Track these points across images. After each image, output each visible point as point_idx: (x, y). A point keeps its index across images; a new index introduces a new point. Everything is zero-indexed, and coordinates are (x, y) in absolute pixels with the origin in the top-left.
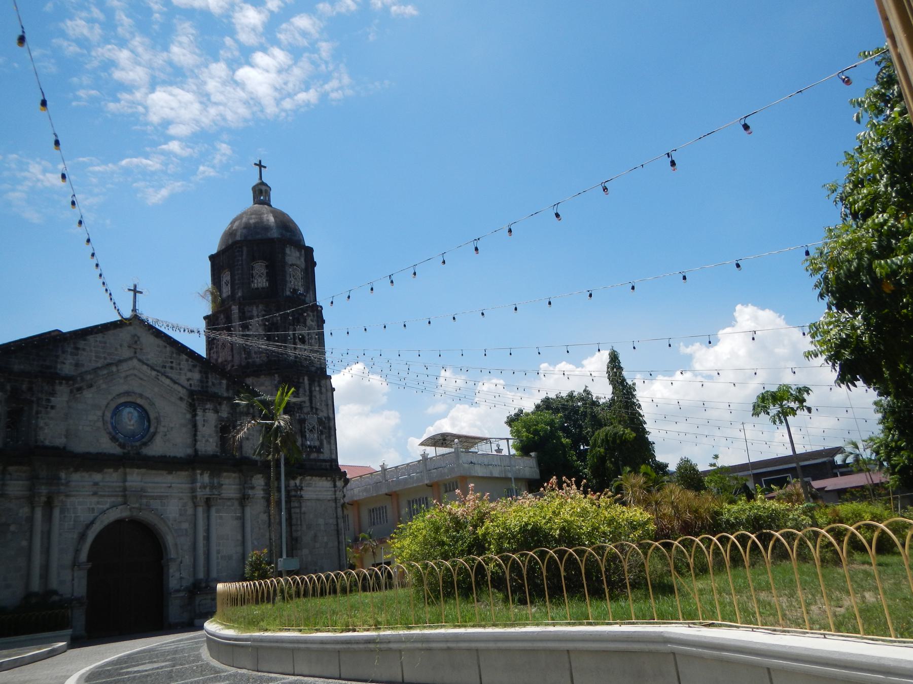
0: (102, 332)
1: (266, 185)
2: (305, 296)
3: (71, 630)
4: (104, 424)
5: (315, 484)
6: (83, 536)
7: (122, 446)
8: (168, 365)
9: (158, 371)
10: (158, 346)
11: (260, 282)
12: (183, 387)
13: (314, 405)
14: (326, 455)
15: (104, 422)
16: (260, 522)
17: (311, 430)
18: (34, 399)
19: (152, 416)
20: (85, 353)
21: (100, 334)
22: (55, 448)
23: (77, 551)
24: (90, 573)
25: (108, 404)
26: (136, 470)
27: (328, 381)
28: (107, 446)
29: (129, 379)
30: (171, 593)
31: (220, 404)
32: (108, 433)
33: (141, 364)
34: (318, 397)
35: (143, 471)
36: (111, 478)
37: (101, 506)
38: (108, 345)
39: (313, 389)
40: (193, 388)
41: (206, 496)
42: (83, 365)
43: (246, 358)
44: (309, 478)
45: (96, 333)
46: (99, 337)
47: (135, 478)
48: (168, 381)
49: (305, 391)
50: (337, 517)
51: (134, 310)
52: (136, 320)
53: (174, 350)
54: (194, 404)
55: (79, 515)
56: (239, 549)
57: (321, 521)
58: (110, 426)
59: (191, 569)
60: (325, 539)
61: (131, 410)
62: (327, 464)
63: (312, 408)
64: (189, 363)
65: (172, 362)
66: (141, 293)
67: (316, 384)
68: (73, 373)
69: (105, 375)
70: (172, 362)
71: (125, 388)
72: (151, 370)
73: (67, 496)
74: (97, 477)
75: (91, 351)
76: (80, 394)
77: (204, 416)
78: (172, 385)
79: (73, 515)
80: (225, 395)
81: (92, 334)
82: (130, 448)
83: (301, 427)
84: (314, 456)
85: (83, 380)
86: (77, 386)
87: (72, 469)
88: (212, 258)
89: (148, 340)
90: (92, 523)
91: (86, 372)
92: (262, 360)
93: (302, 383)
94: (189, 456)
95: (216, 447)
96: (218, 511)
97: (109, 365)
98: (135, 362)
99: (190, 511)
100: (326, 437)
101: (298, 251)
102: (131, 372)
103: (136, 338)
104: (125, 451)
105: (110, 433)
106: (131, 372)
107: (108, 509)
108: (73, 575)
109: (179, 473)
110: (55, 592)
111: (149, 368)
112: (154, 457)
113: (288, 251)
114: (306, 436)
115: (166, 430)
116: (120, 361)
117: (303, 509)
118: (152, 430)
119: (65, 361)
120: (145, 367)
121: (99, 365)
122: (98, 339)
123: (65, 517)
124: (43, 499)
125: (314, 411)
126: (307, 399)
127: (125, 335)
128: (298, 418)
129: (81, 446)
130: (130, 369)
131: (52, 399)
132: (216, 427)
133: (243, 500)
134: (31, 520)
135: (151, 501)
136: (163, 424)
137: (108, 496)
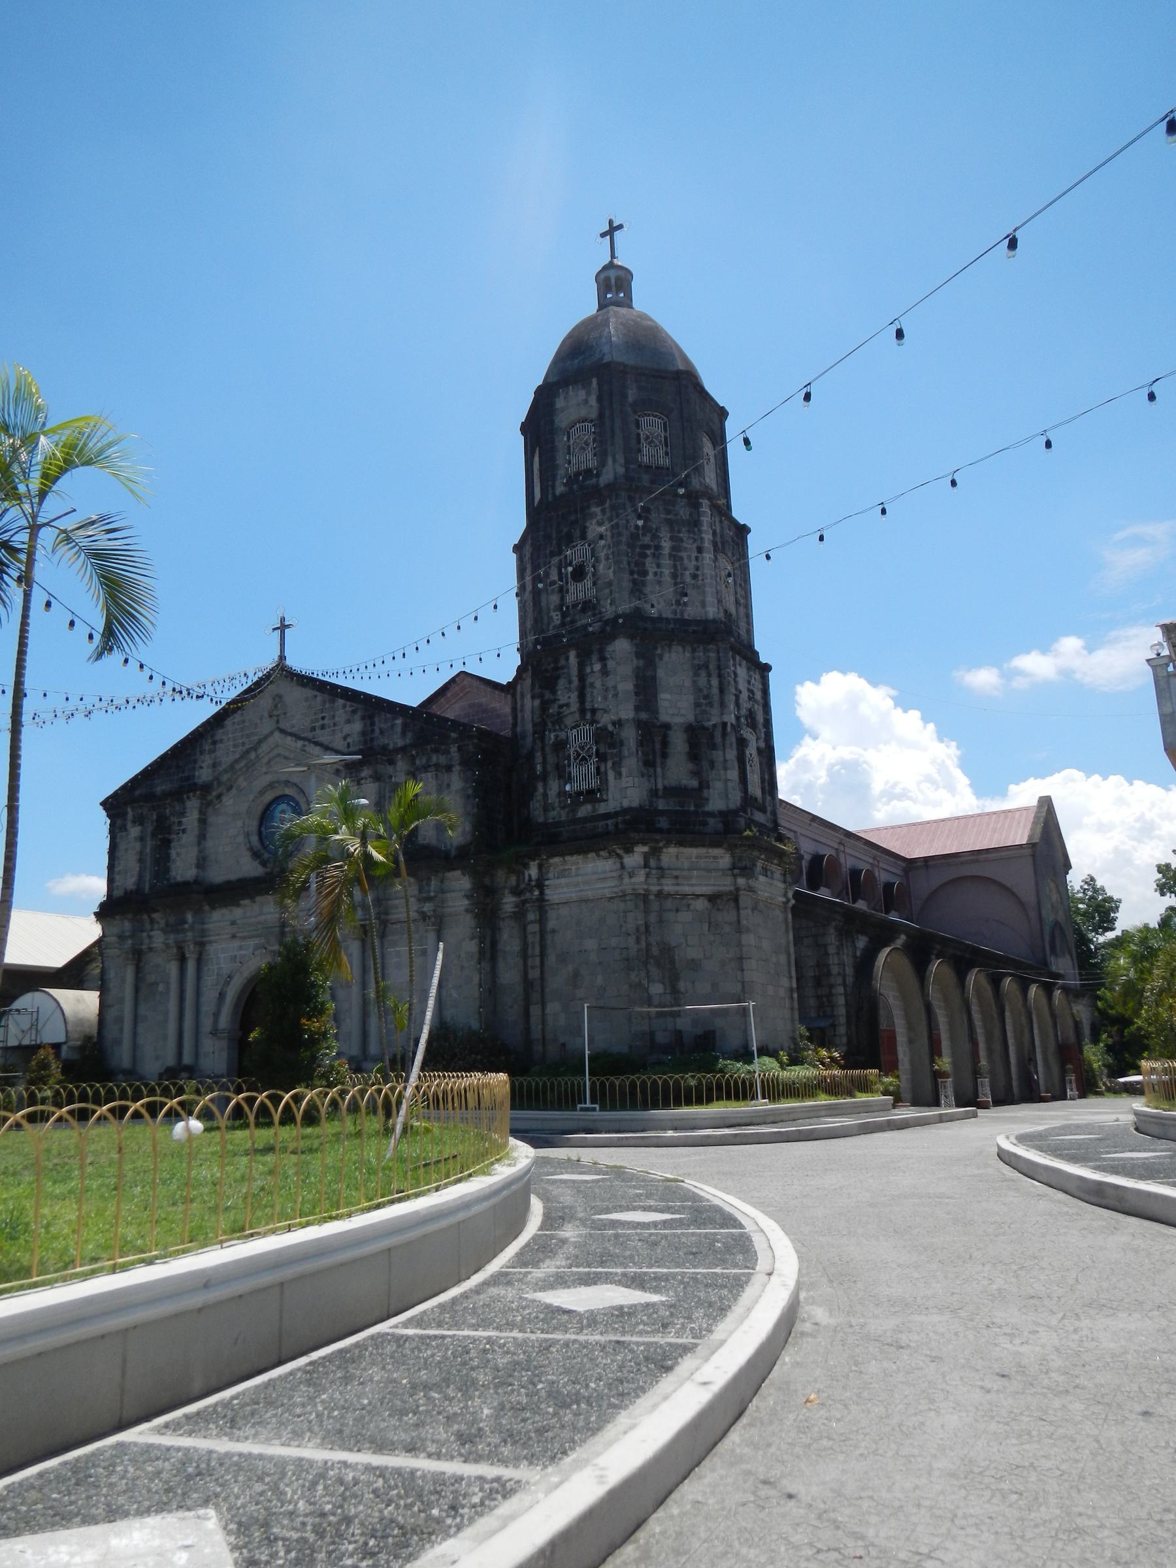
2: (598, 475)
5: (578, 869)
6: (222, 996)
7: (264, 864)
10: (307, 699)
13: (588, 706)
17: (584, 759)
20: (222, 746)
22: (186, 884)
23: (216, 1015)
28: (249, 868)
31: (392, 762)
34: (598, 684)
37: (243, 952)
39: (588, 670)
44: (556, 860)
46: (237, 717)
49: (570, 682)
51: (282, 657)
52: (282, 672)
53: (326, 696)
57: (591, 944)
58: (255, 839)
60: (599, 980)
62: (609, 822)
63: (582, 711)
65: (323, 718)
66: (288, 626)
67: (595, 658)
68: (210, 778)
71: (268, 778)
74: (237, 913)
80: (400, 743)
81: (229, 716)
83: (558, 756)
84: (584, 811)
85: (219, 784)
86: (214, 794)
87: (207, 908)
89: (294, 695)
93: (562, 668)
98: (277, 734)
100: (614, 764)
101: (584, 388)
102: (276, 752)
104: (268, 870)
105: (251, 849)
106: (276, 752)
116: (260, 742)
117: (551, 924)
120: (289, 738)
121: (237, 756)
125: (588, 716)
126: (574, 696)
127: (264, 702)
129: (218, 875)
130: (272, 750)
131: (183, 820)
137: (251, 937)
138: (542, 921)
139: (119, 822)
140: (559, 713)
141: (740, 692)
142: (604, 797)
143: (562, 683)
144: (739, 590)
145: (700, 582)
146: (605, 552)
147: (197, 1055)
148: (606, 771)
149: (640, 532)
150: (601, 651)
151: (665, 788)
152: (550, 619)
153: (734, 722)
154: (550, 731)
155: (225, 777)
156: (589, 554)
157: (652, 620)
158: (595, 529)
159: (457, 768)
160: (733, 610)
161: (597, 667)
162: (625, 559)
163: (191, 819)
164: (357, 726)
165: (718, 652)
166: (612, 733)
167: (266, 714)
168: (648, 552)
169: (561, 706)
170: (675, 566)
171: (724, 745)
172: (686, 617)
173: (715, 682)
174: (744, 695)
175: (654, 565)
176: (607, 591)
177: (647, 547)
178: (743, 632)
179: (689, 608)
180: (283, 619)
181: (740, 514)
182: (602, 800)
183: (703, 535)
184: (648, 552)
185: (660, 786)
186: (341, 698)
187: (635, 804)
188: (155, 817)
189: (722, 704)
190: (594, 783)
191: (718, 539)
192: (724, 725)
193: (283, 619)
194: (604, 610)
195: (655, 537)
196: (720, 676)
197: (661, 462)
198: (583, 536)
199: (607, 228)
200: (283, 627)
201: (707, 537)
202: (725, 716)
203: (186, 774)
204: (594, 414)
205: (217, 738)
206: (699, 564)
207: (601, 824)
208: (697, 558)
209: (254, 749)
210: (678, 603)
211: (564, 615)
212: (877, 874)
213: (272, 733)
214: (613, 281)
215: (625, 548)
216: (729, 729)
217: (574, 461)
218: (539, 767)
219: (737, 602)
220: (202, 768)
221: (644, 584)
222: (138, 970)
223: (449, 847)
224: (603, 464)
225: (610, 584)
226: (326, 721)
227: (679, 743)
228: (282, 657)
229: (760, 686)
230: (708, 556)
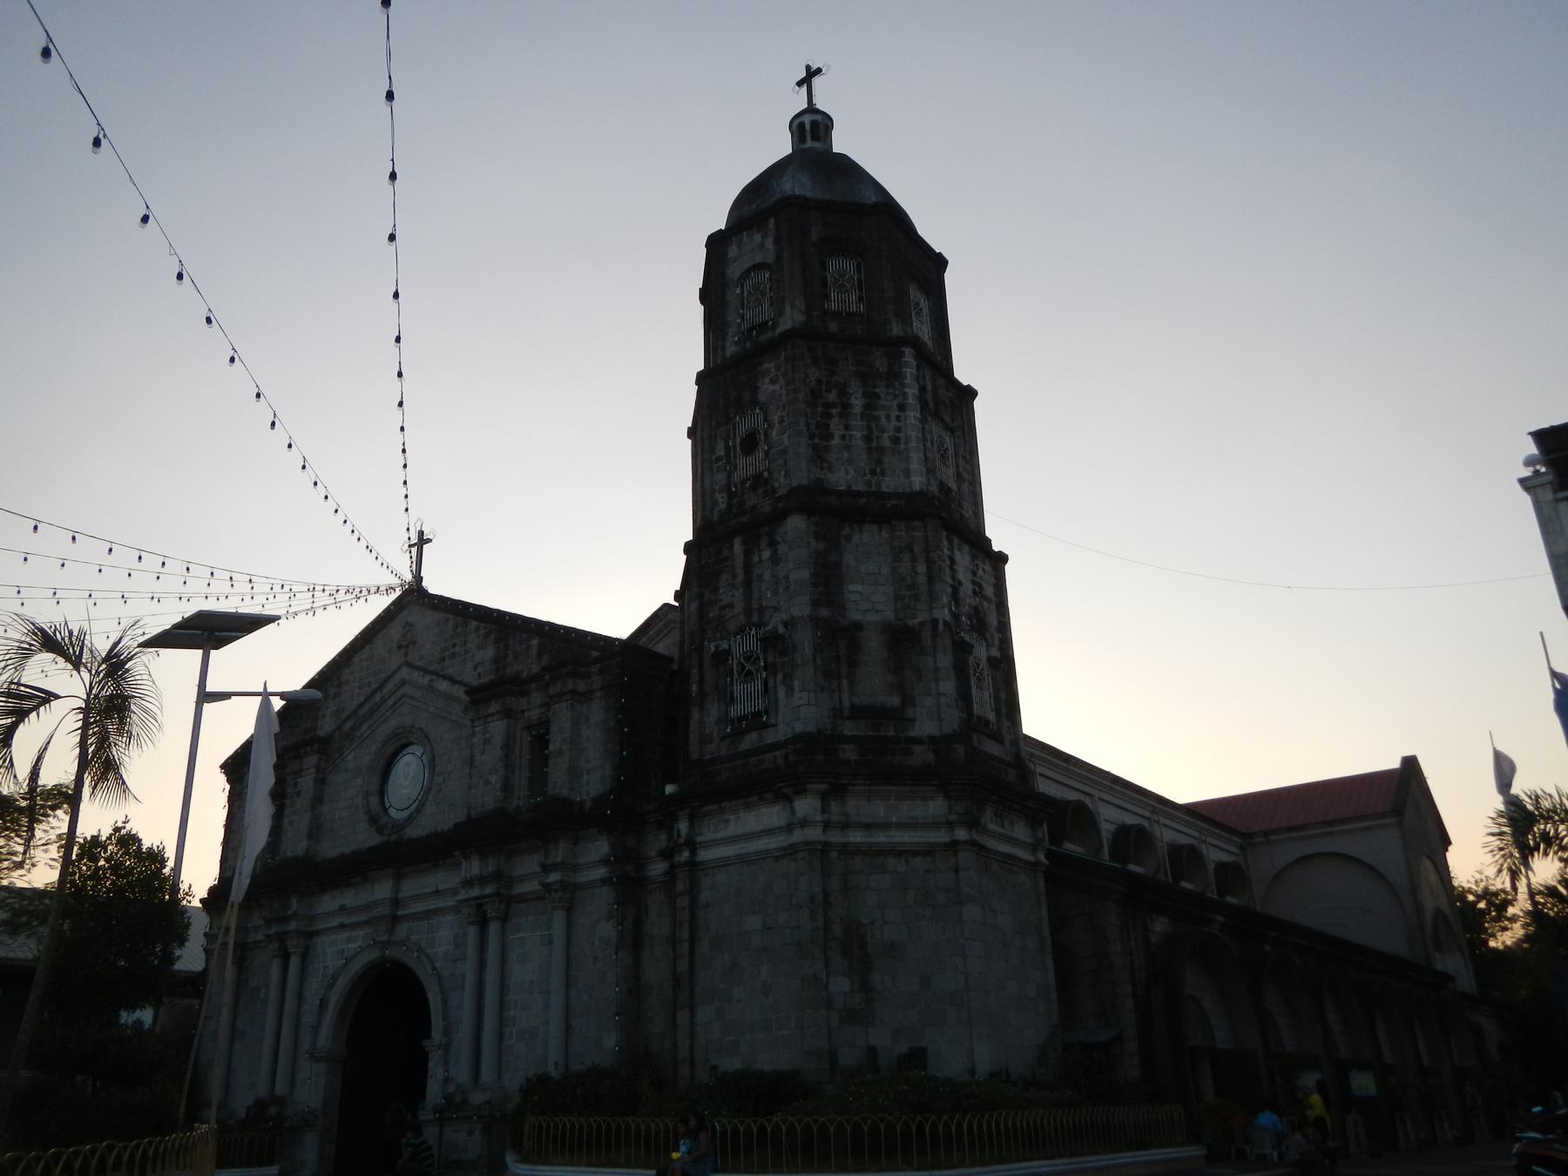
2: (774, 327)
3: (278, 1167)
7: (380, 830)
8: (448, 653)
17: (749, 673)
23: (316, 1028)
34: (767, 576)
39: (756, 559)
40: (484, 680)
45: (362, 647)
46: (365, 653)
47: (382, 890)
48: (443, 686)
49: (734, 576)
58: (374, 800)
62: (777, 753)
63: (748, 610)
65: (454, 645)
67: (763, 542)
71: (392, 723)
72: (423, 676)
80: (535, 669)
84: (750, 740)
95: (507, 787)
98: (405, 673)
100: (784, 676)
104: (385, 838)
120: (416, 673)
121: (362, 699)
125: (755, 618)
126: (738, 593)
127: (394, 631)
129: (330, 849)
131: (299, 780)
138: (693, 892)
141: (960, 583)
142: (773, 721)
143: (725, 578)
144: (961, 462)
145: (903, 446)
146: (779, 414)
147: (292, 1083)
148: (775, 687)
149: (824, 388)
151: (853, 706)
152: (715, 503)
153: (948, 617)
154: (710, 642)
156: (761, 418)
157: (839, 494)
158: (767, 388)
159: (598, 694)
160: (954, 487)
161: (766, 554)
162: (803, 419)
164: (490, 652)
165: (926, 531)
166: (783, 637)
168: (834, 411)
169: (723, 608)
170: (869, 428)
171: (934, 649)
172: (884, 489)
173: (922, 568)
174: (967, 588)
175: (841, 427)
176: (781, 462)
177: (834, 405)
178: (968, 513)
179: (887, 479)
180: (421, 533)
181: (963, 373)
182: (766, 726)
183: (906, 390)
184: (834, 411)
185: (846, 702)
187: (811, 727)
189: (932, 597)
190: (760, 706)
191: (929, 396)
192: (935, 622)
193: (421, 533)
194: (777, 485)
195: (843, 393)
196: (928, 561)
197: (854, 308)
198: (754, 402)
199: (803, 74)
200: (422, 541)
201: (912, 391)
202: (935, 611)
204: (770, 259)
206: (901, 424)
207: (767, 756)
208: (898, 418)
209: (380, 688)
210: (873, 472)
211: (731, 496)
212: (1205, 852)
213: (399, 669)
214: (808, 127)
215: (803, 406)
216: (941, 626)
217: (748, 315)
218: (694, 688)
219: (959, 476)
221: (827, 449)
223: (585, 798)
224: (780, 313)
225: (785, 452)
226: (457, 649)
227: (873, 644)
228: (418, 578)
229: (993, 580)
230: (913, 415)
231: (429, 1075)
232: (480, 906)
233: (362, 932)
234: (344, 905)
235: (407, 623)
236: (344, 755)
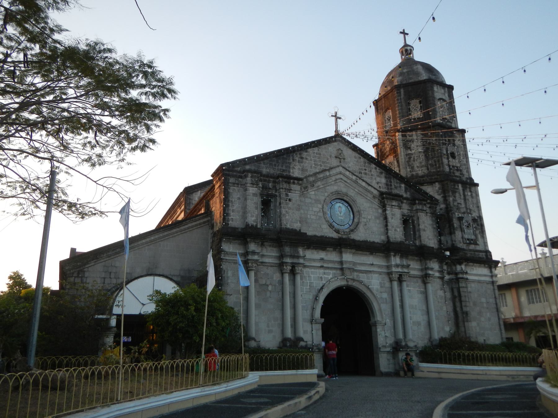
0: (317, 146)
1: (410, 46)
2: (451, 123)
4: (324, 215)
6: (316, 299)
7: (337, 231)
9: (357, 176)
10: (355, 157)
11: (417, 114)
12: (375, 188)
14: (480, 247)
15: (324, 213)
16: (438, 297)
17: (468, 227)
18: (277, 194)
19: (355, 210)
20: (307, 162)
21: (316, 148)
24: (323, 325)
25: (325, 199)
26: (349, 250)
27: (476, 187)
29: (338, 181)
30: (380, 348)
31: (402, 203)
32: (326, 221)
33: (345, 170)
34: (470, 199)
35: (354, 251)
36: (332, 256)
37: (326, 276)
38: (322, 156)
39: (466, 194)
40: (381, 190)
41: (399, 273)
42: (307, 170)
43: (410, 172)
45: (314, 147)
46: (316, 150)
47: (348, 257)
48: (364, 184)
50: (495, 298)
52: (338, 138)
53: (366, 161)
54: (384, 201)
55: (312, 281)
56: (425, 317)
57: (484, 300)
59: (392, 330)
61: (341, 205)
63: (467, 209)
64: (377, 170)
67: (468, 190)
68: (300, 176)
69: (322, 177)
70: (365, 170)
71: (335, 188)
73: (305, 266)
74: (322, 255)
75: (311, 160)
76: (306, 191)
77: (391, 211)
78: (367, 186)
79: (308, 281)
80: (405, 196)
81: (311, 147)
82: (342, 233)
84: (472, 247)
87: (306, 247)
88: (376, 103)
89: (348, 153)
90: (322, 288)
91: (310, 176)
92: (424, 172)
93: (457, 189)
94: (384, 241)
96: (407, 286)
97: (324, 170)
98: (341, 169)
99: (387, 284)
100: (480, 232)
101: (443, 89)
103: (340, 152)
104: (340, 235)
107: (331, 278)
108: (312, 328)
109: (377, 254)
110: (301, 339)
111: (351, 174)
112: (359, 241)
113: (435, 89)
114: (464, 231)
115: (365, 220)
118: (356, 220)
119: (295, 167)
121: (318, 171)
122: (315, 152)
123: (303, 282)
124: (289, 268)
126: (462, 202)
127: (332, 148)
128: (457, 216)
132: (400, 219)
133: (425, 278)
134: (282, 283)
135: (360, 274)
136: (363, 216)
139: (232, 180)
140: (458, 206)
143: (457, 195)
150: (470, 188)
155: (311, 179)
159: (429, 214)
163: (295, 195)
167: (333, 156)
169: (458, 203)
186: (374, 164)
188: (261, 186)
194: (464, 173)
203: (284, 168)
205: (304, 156)
218: (455, 225)
220: (294, 168)
222: (256, 274)
231: (378, 334)
232: (400, 275)
233: (331, 272)
234: (323, 258)
235: (340, 149)
236: (309, 191)
